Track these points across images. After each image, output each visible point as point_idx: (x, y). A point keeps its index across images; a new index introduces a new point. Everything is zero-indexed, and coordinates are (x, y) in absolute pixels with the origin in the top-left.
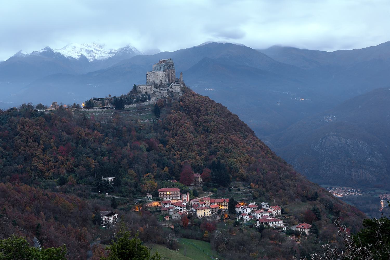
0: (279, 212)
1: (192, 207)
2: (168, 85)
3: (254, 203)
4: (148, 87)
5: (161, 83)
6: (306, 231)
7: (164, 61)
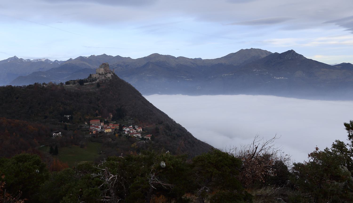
0: (141, 130)
1: (103, 128)
2: (106, 74)
3: (132, 126)
4: (96, 75)
5: (102, 73)
6: (150, 138)
7: (104, 64)
